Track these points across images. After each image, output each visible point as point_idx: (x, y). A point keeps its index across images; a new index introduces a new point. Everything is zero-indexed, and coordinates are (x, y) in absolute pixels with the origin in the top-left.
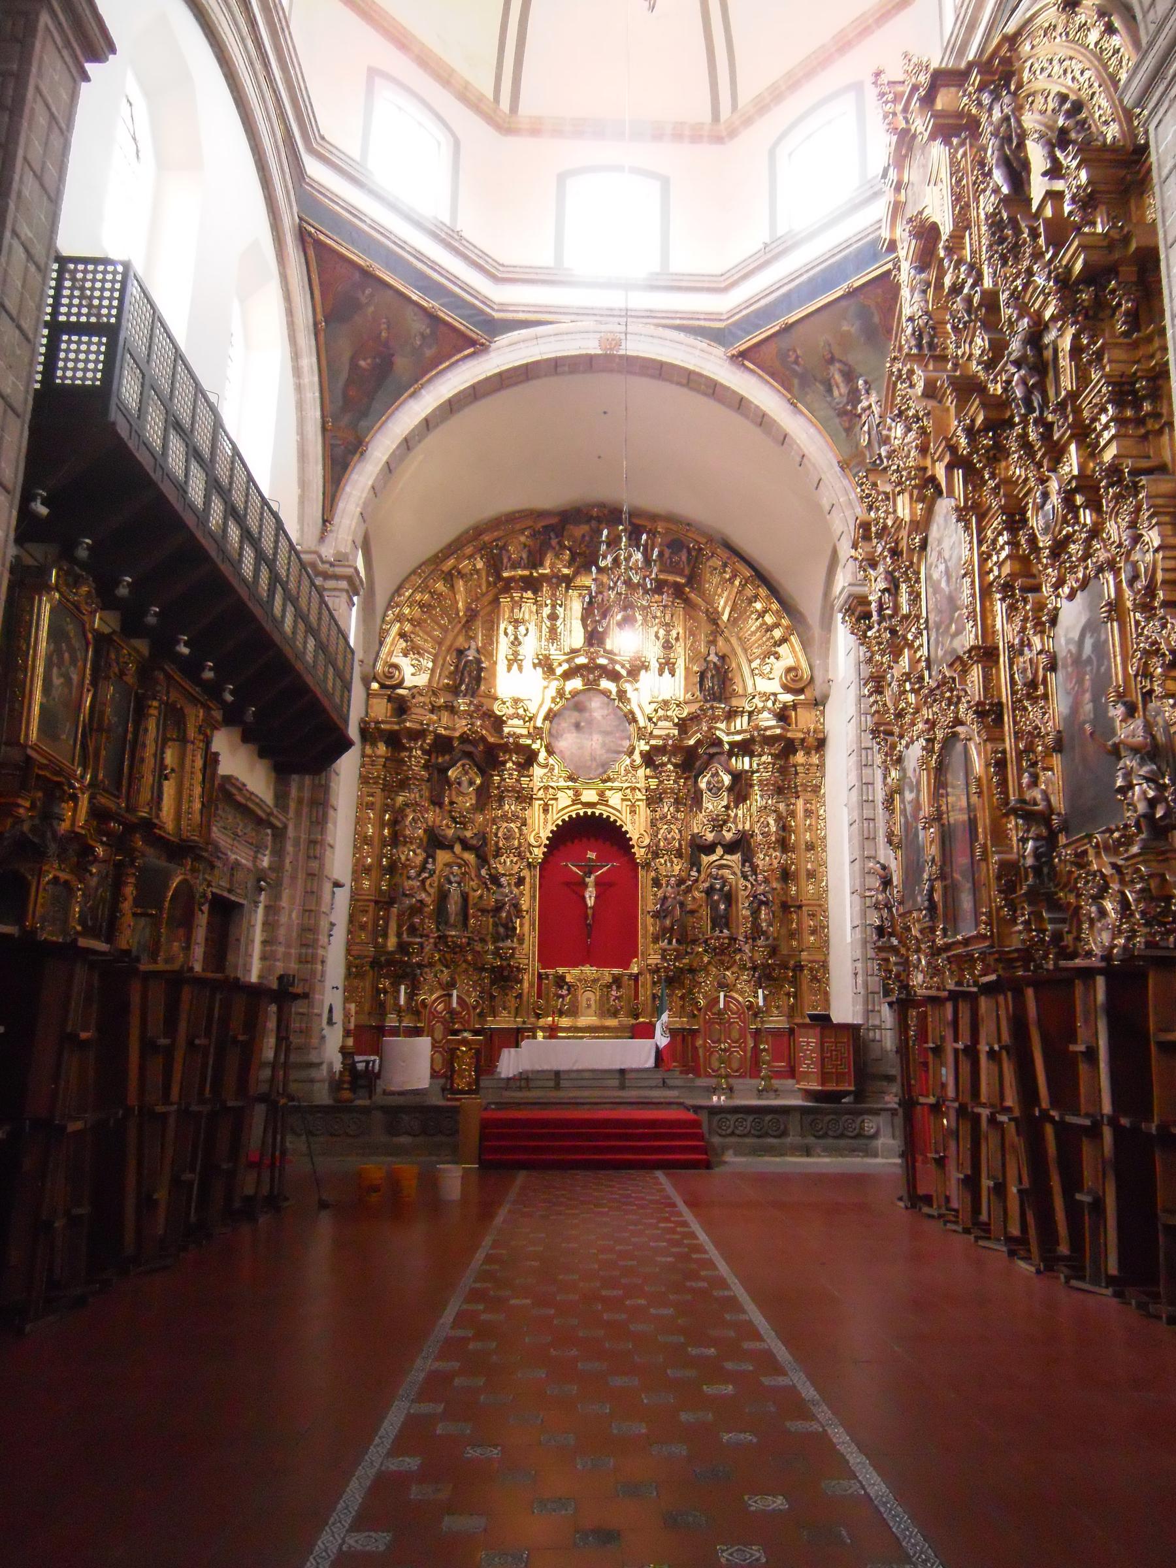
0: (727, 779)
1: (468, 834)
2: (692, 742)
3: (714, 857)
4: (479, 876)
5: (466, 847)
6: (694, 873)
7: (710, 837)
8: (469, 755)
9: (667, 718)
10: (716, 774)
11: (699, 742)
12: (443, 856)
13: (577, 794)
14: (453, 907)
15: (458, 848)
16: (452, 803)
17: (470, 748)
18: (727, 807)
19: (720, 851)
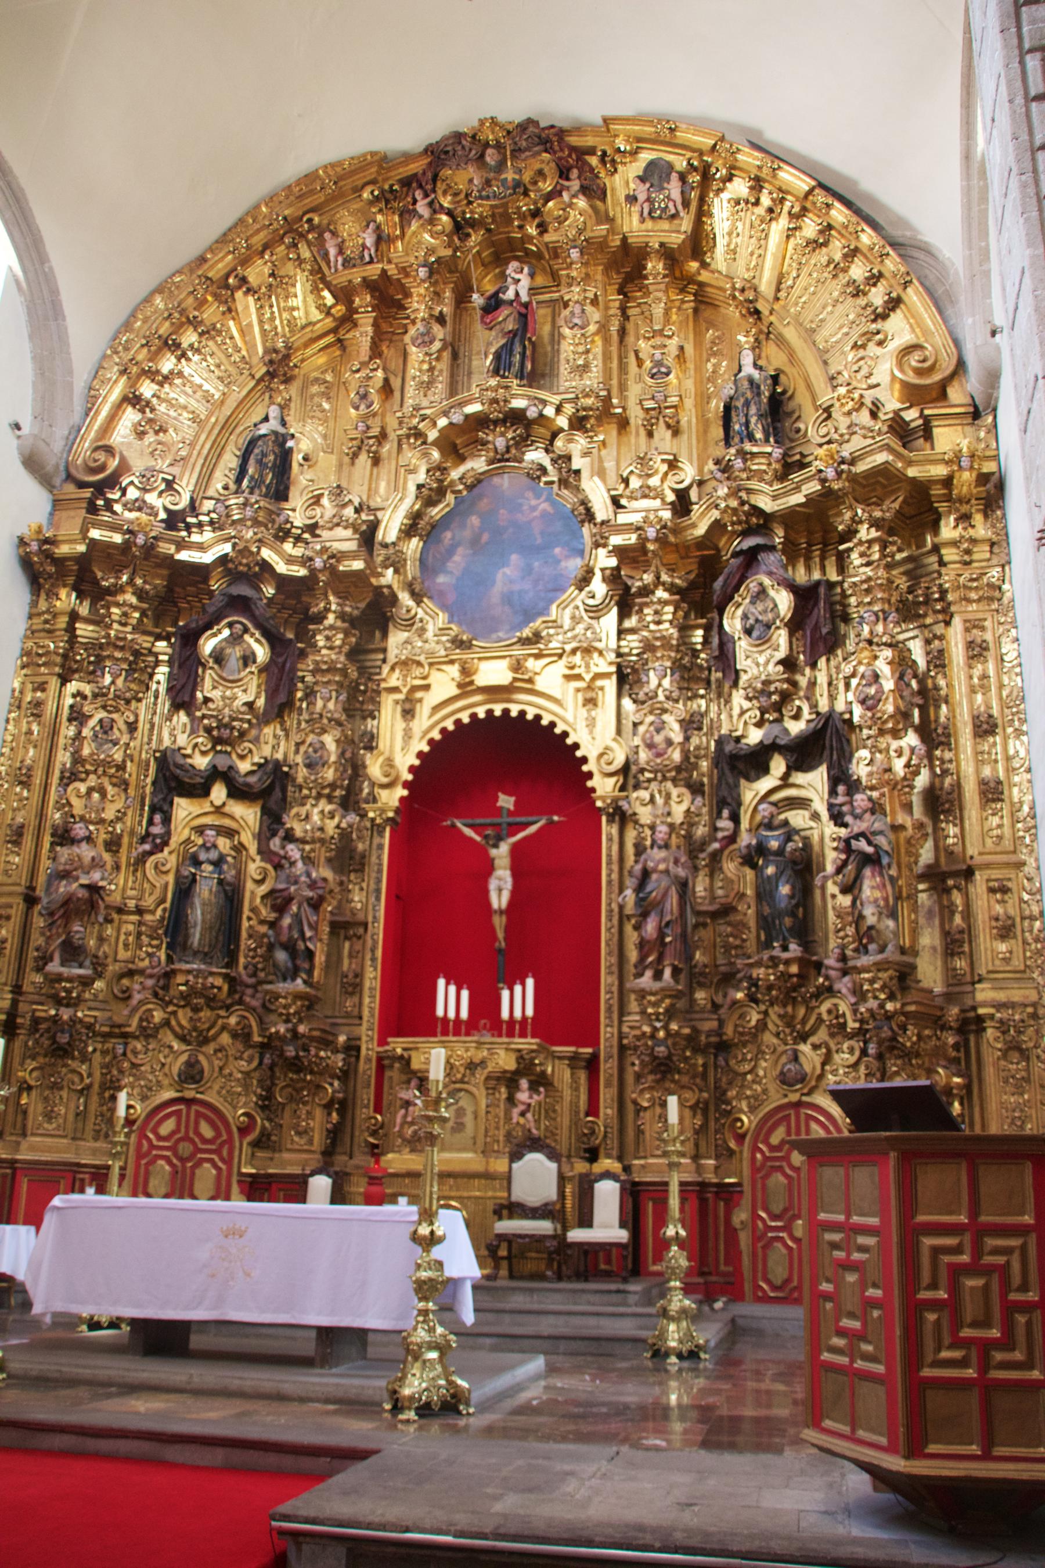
0: (784, 601)
1: (244, 767)
2: (701, 530)
3: (765, 784)
4: (264, 852)
5: (238, 792)
6: (725, 824)
7: (755, 736)
8: (241, 604)
9: (646, 492)
10: (762, 593)
11: (717, 526)
12: (184, 809)
13: (465, 671)
14: (198, 914)
15: (219, 793)
16: (207, 700)
17: (243, 590)
18: (789, 664)
19: (778, 765)
